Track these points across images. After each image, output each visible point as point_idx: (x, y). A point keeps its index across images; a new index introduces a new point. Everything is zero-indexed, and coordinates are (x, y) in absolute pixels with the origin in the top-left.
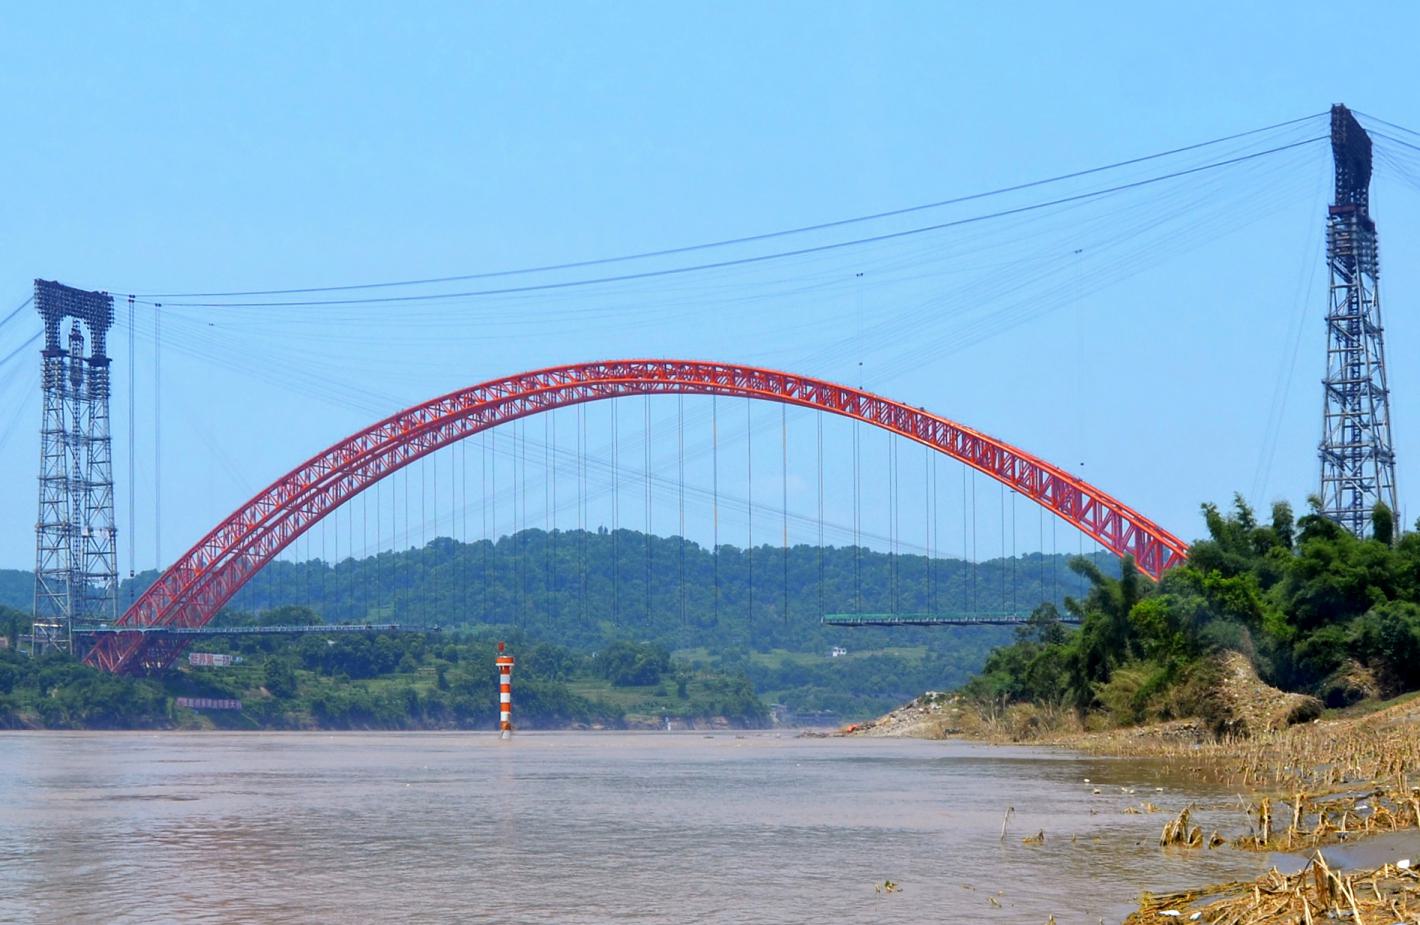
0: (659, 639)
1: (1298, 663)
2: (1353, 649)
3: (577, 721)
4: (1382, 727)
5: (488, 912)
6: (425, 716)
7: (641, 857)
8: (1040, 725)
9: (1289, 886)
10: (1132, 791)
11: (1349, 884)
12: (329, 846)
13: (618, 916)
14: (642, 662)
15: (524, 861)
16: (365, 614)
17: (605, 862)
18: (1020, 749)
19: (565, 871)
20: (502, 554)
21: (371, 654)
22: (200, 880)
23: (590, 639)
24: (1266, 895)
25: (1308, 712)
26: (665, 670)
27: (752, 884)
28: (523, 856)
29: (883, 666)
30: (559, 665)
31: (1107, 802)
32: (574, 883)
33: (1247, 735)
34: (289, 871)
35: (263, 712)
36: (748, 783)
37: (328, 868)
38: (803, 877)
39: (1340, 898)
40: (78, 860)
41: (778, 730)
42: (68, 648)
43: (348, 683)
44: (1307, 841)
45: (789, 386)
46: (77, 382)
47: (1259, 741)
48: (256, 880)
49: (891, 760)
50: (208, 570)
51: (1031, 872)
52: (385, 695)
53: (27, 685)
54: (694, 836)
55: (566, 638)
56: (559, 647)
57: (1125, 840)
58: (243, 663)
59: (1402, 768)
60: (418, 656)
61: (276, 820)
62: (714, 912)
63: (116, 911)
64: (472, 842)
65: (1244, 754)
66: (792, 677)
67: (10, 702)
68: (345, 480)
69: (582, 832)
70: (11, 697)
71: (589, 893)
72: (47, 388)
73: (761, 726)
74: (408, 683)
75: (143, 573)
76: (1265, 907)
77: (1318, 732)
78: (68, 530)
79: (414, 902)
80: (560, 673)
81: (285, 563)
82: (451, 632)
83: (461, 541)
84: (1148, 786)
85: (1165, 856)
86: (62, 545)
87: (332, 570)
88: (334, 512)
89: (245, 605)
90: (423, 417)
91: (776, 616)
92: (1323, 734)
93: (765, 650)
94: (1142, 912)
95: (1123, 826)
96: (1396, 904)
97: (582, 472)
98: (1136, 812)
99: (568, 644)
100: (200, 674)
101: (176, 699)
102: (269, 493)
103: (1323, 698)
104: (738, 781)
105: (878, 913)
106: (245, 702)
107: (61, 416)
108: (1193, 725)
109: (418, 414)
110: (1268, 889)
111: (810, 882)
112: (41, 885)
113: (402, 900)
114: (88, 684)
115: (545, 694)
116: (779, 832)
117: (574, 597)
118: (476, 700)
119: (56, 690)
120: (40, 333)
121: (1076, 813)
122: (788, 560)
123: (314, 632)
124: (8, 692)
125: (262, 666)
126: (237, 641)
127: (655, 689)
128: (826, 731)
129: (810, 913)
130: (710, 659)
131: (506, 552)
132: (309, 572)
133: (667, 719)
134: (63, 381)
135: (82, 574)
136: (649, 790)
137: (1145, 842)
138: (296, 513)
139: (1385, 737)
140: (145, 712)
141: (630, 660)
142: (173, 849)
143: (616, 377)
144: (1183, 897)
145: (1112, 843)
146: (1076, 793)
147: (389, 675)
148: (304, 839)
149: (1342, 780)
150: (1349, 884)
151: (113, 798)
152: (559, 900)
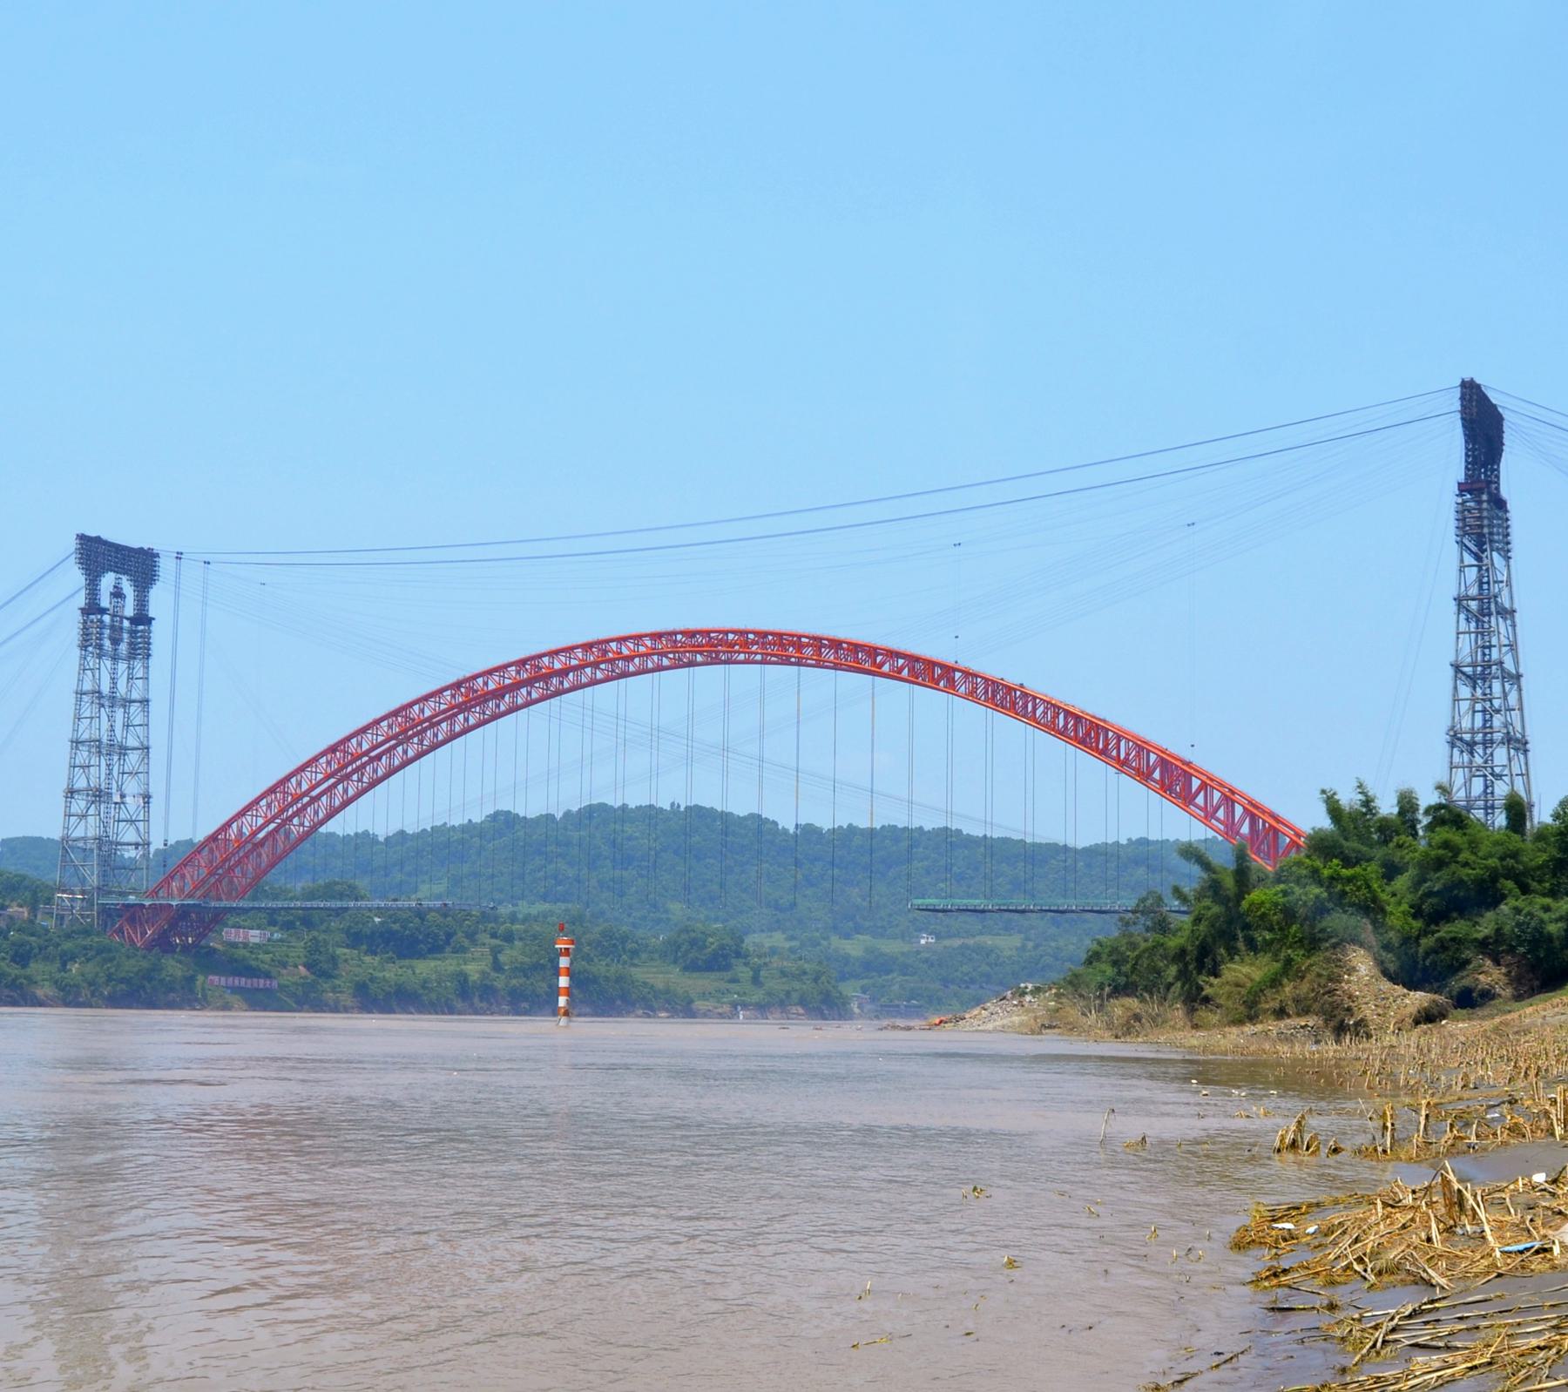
0: (732, 923)
1: (1424, 960)
2: (1483, 946)
3: (642, 1009)
4: (1516, 1029)
5: (537, 1212)
6: (476, 1000)
7: (706, 1155)
8: (1144, 1020)
9: (1414, 1199)
10: (1243, 1094)
11: (1479, 1198)
12: (367, 1137)
13: (679, 1219)
14: (713, 947)
15: (579, 1158)
16: (416, 890)
17: (668, 1160)
18: (1122, 1046)
19: (623, 1169)
20: (566, 829)
21: (420, 933)
22: (224, 1172)
23: (659, 921)
24: (1389, 1209)
25: (1435, 1012)
26: (738, 955)
27: (828, 1187)
28: (578, 1152)
29: (974, 955)
30: (623, 948)
31: (1216, 1105)
32: (632, 1182)
33: (1369, 1036)
34: (322, 1164)
35: (300, 992)
36: (827, 1078)
37: (364, 1162)
38: (883, 1180)
39: (1470, 1213)
40: (93, 1148)
41: (859, 1022)
42: (93, 920)
43: (394, 963)
44: (1434, 1151)
45: (879, 659)
46: (116, 642)
47: (1382, 1043)
48: (286, 1173)
49: (982, 1055)
50: (246, 842)
51: (1133, 1180)
52: (434, 977)
53: (46, 959)
54: (765, 1134)
55: (631, 920)
56: (624, 928)
57: (1236, 1146)
58: (281, 940)
59: (1537, 1075)
60: (471, 936)
61: (309, 1108)
62: (784, 1216)
63: (130, 1204)
64: (523, 1136)
65: (1365, 1056)
66: (875, 966)
67: (26, 978)
68: (400, 749)
69: (642, 1127)
70: (28, 971)
71: (649, 1194)
72: (84, 647)
73: (841, 1017)
74: (459, 964)
75: (177, 842)
76: (1388, 1221)
77: (1446, 1033)
78: (99, 795)
79: (457, 1200)
80: (624, 957)
81: (332, 835)
82: (508, 911)
83: (522, 815)
84: (1260, 1089)
85: (1278, 1164)
86: (90, 812)
87: (381, 843)
88: (386, 781)
89: (286, 878)
90: (486, 684)
91: (859, 900)
92: (1451, 1036)
93: (847, 936)
94: (1253, 1224)
95: (1233, 1131)
96: (1532, 1220)
97: (655, 744)
98: (1248, 1117)
99: (634, 925)
100: (234, 950)
101: (207, 978)
102: (317, 761)
103: (1451, 998)
104: (815, 1075)
105: (964, 1221)
106: (282, 982)
107: (97, 676)
108: (1310, 1024)
109: (480, 680)
110: (1391, 1202)
111: (890, 1186)
112: (51, 1174)
113: (444, 1197)
114: (111, 960)
115: (607, 979)
116: (857, 1131)
117: (642, 876)
118: (532, 984)
119: (77, 965)
120: (80, 590)
121: (1182, 1116)
122: (874, 841)
123: (359, 908)
124: (24, 966)
125: (302, 944)
126: (275, 916)
127: (728, 975)
128: (911, 1024)
129: (890, 1219)
130: (787, 945)
131: (570, 827)
132: (356, 844)
133: (739, 1008)
134: (101, 639)
135: (111, 843)
136: (717, 1083)
137: (1257, 1149)
138: (345, 783)
139: (1518, 1040)
140: (172, 990)
141: (700, 943)
142: (195, 1138)
143: (694, 646)
144: (1298, 1208)
145: (1221, 1149)
146: (1182, 1095)
147: (438, 956)
148: (340, 1130)
149: (1472, 1086)
150: (1479, 1198)
151: (134, 1082)
152: (615, 1201)
